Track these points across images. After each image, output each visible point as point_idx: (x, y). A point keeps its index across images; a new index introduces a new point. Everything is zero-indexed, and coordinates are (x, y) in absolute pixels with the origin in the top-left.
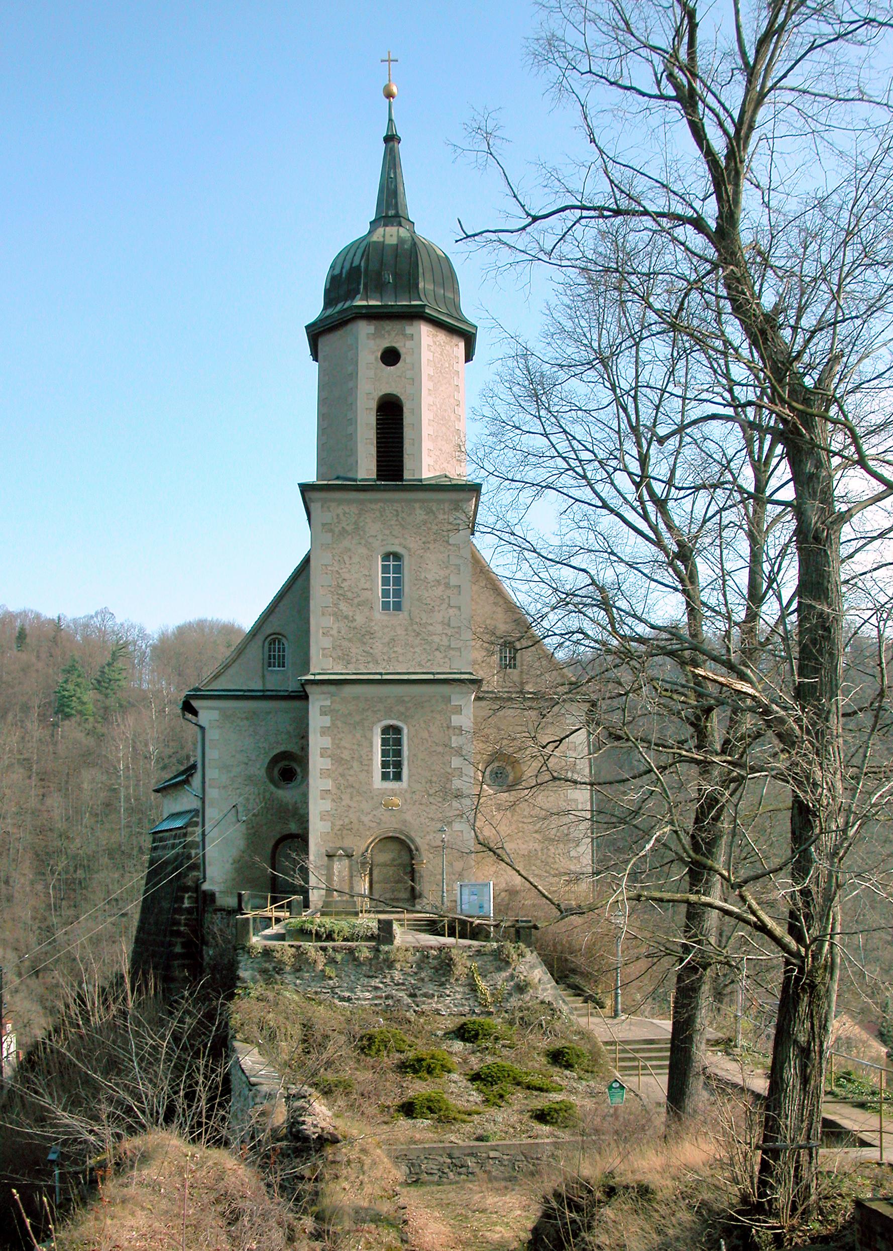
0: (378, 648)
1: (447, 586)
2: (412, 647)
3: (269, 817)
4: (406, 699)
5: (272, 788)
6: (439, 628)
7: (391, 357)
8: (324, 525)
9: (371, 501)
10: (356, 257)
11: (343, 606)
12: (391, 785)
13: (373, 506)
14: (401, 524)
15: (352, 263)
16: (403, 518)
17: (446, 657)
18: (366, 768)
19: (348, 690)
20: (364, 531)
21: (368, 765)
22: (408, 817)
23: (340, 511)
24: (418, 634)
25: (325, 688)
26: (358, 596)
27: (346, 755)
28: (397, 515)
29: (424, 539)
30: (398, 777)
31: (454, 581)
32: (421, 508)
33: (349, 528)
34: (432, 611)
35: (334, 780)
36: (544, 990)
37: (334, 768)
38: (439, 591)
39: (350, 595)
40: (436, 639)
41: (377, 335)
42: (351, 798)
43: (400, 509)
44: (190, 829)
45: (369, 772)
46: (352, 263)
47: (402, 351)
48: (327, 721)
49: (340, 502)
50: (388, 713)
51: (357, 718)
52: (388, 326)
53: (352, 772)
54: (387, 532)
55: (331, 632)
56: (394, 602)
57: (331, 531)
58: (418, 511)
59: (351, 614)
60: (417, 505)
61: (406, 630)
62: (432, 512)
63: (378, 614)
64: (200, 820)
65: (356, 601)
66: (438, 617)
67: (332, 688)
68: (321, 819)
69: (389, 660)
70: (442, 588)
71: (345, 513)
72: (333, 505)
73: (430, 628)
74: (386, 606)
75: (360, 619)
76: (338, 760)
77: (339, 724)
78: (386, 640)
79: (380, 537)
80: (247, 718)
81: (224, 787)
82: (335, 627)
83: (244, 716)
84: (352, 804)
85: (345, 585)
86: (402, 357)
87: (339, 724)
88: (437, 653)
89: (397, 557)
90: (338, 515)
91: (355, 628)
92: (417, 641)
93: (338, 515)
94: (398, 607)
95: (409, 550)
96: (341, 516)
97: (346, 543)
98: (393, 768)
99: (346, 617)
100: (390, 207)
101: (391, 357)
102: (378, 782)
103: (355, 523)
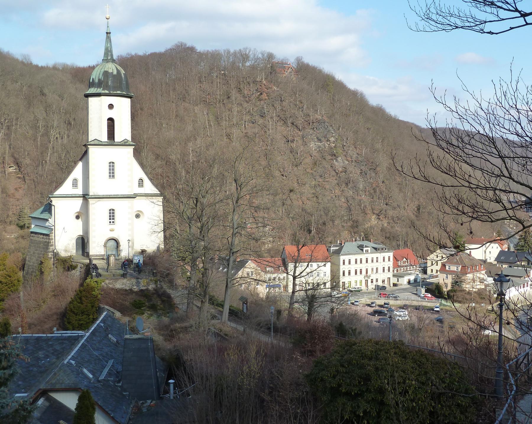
7: (111, 106)
56: (112, 175)
101: (111, 106)
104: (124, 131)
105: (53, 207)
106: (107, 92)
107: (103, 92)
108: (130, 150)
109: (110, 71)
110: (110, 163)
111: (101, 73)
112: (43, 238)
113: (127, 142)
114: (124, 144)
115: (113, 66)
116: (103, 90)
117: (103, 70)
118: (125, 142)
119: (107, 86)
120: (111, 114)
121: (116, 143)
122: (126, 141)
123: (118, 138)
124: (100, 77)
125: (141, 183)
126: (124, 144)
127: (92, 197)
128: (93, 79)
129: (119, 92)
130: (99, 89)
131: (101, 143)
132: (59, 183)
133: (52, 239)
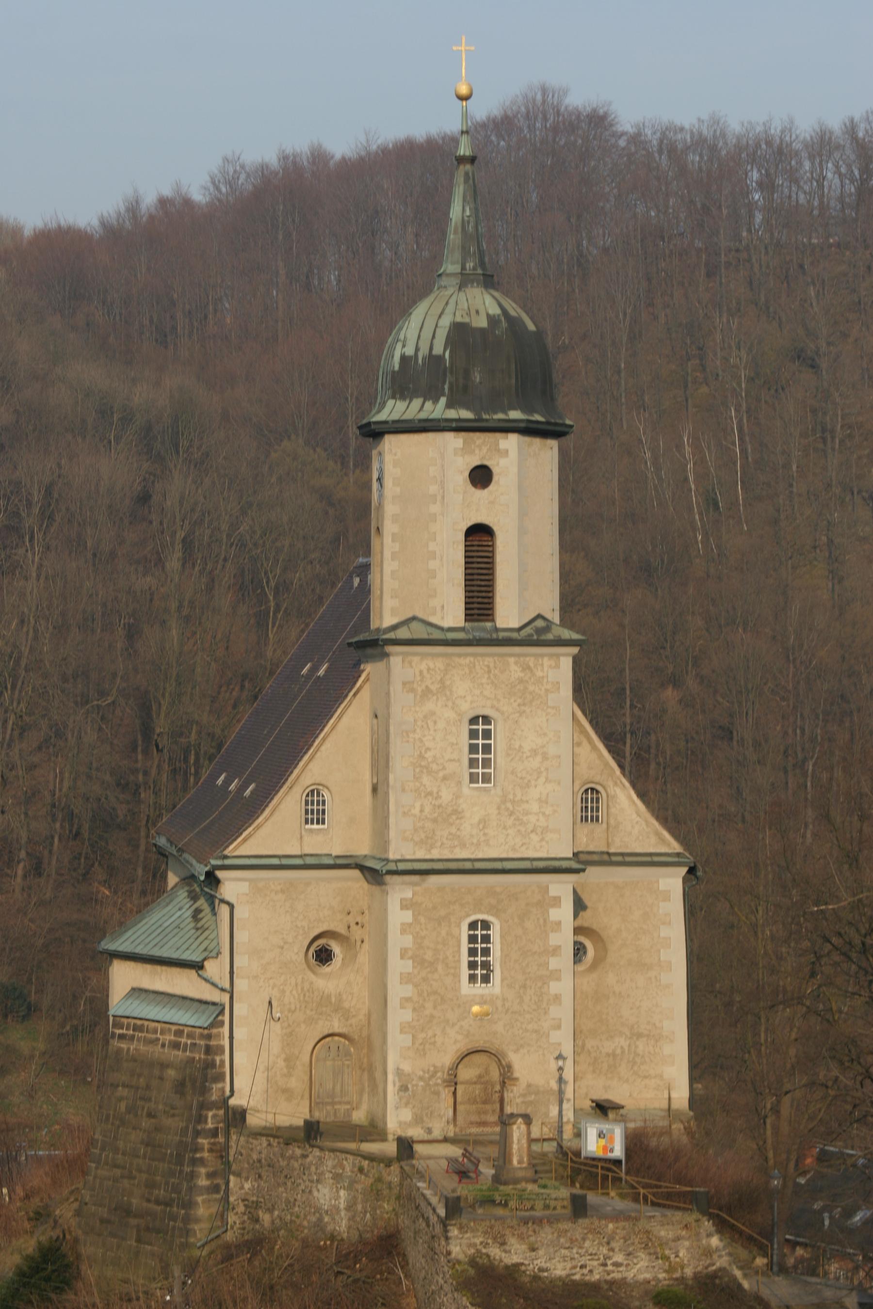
1: (545, 757)
2: (505, 828)
3: (308, 1012)
4: (498, 890)
5: (312, 976)
6: (535, 807)
7: (481, 476)
8: (404, 684)
9: (459, 655)
10: (435, 342)
11: (426, 780)
12: (479, 988)
13: (462, 661)
14: (493, 683)
15: (431, 348)
16: (495, 676)
17: (542, 840)
18: (452, 971)
19: (434, 879)
20: (451, 691)
22: (499, 1027)
23: (423, 666)
24: (511, 814)
25: (407, 878)
26: (444, 768)
27: (429, 956)
28: (489, 672)
29: (519, 701)
30: (486, 979)
31: (552, 750)
32: (516, 663)
33: (434, 688)
34: (528, 785)
35: (416, 986)
36: (720, 1257)
37: (416, 972)
38: (535, 763)
39: (434, 767)
40: (533, 819)
41: (466, 450)
42: (435, 1007)
43: (492, 665)
44: (214, 1031)
45: (457, 976)
46: (431, 348)
47: (495, 470)
48: (407, 916)
49: (424, 656)
51: (443, 912)
54: (477, 692)
55: (413, 811)
57: (413, 690)
58: (513, 667)
59: (435, 790)
60: (512, 660)
61: (499, 808)
62: (529, 668)
63: (467, 789)
64: (226, 1018)
65: (441, 774)
67: (415, 878)
68: (401, 1032)
69: (478, 844)
70: (539, 758)
71: (429, 669)
72: (416, 659)
73: (525, 806)
74: (473, 778)
75: (446, 795)
76: (419, 961)
77: (422, 920)
78: (476, 820)
79: (469, 698)
80: (282, 891)
81: (256, 977)
82: (418, 805)
83: (279, 888)
85: (429, 755)
86: (495, 478)
87: (422, 920)
88: (533, 836)
89: (486, 720)
90: (421, 672)
91: (440, 806)
92: (510, 822)
93: (421, 672)
95: (502, 713)
96: (425, 672)
97: (430, 705)
98: (480, 971)
99: (430, 794)
101: (481, 476)
103: (442, 681)
105: (224, 910)
106: (466, 414)
107: (452, 414)
108: (557, 670)
109: (481, 322)
110: (474, 720)
114: (534, 636)
115: (488, 300)
116: (449, 405)
118: (539, 631)
119: (465, 388)
120: (481, 507)
121: (502, 635)
122: (540, 623)
123: (508, 614)
124: (438, 350)
125: (590, 804)
126: (534, 636)
127: (402, 866)
128: (404, 358)
129: (515, 414)
131: (437, 635)
132: (249, 811)
133: (221, 1050)
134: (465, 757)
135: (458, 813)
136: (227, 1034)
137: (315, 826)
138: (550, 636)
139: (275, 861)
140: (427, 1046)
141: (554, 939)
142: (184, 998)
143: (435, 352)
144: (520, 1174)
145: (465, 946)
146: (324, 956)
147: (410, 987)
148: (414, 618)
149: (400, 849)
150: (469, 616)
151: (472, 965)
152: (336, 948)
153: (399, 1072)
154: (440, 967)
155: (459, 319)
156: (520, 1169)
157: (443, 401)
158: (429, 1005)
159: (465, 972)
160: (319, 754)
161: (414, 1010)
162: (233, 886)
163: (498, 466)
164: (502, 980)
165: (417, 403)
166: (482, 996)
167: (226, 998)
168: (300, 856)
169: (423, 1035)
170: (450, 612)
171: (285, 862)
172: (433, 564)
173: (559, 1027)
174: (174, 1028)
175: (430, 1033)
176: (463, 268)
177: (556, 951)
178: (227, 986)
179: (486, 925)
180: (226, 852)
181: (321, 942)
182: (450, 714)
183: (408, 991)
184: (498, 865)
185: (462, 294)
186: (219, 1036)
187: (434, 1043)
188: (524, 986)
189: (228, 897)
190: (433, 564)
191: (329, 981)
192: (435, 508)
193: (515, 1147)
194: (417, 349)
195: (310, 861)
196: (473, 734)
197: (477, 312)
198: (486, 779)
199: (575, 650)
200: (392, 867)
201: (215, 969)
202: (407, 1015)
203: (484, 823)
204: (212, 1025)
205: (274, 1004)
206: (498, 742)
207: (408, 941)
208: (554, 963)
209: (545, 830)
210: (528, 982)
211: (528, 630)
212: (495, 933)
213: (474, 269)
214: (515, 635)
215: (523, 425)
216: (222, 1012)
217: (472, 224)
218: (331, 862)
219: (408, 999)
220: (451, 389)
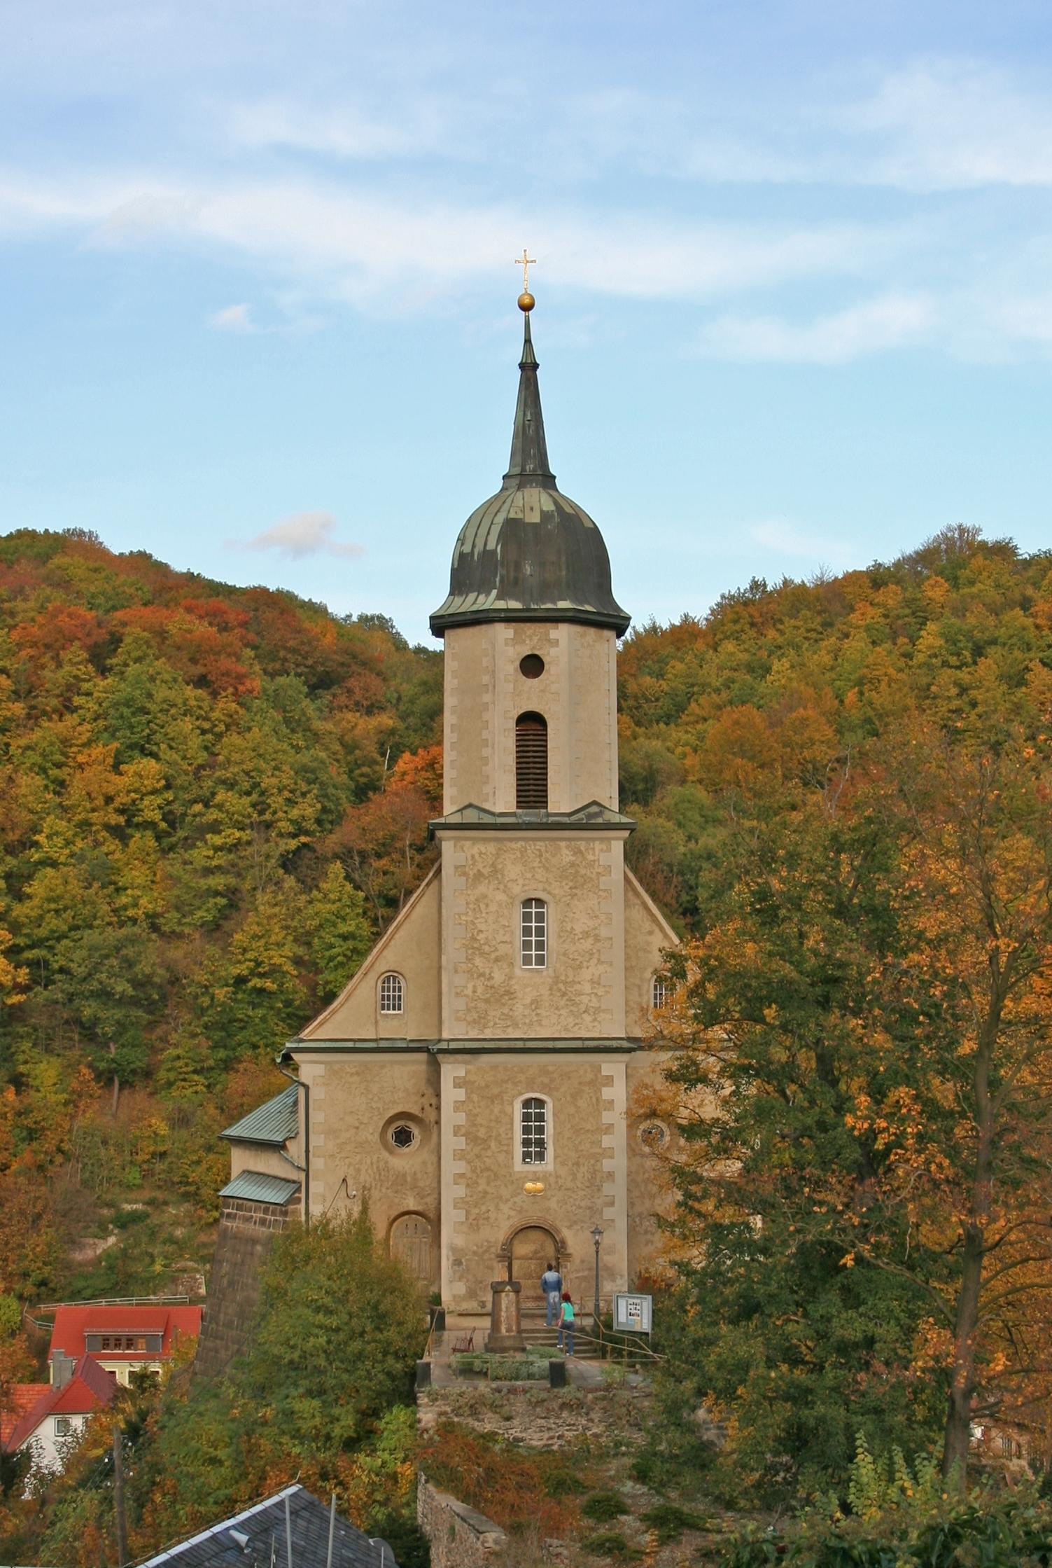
0: (519, 1010)
1: (597, 939)
2: (557, 1008)
3: (384, 1190)
4: (551, 1069)
6: (587, 988)
7: (532, 666)
8: (456, 867)
9: (511, 840)
10: (490, 538)
11: (478, 961)
12: (536, 1166)
13: (513, 845)
14: (544, 866)
15: (485, 544)
16: (547, 859)
17: (595, 1020)
19: (485, 1058)
20: (503, 875)
21: (508, 1145)
22: (553, 1204)
23: (475, 851)
24: (564, 994)
25: (459, 1057)
26: (496, 950)
27: (482, 1133)
28: (541, 856)
29: (571, 884)
30: (541, 1156)
31: (604, 932)
32: (567, 847)
33: (485, 871)
34: (580, 967)
35: (469, 1162)
38: (587, 944)
39: (486, 948)
40: (585, 999)
41: (516, 640)
42: (488, 1183)
43: (543, 849)
45: (510, 1153)
46: (485, 544)
47: (545, 659)
48: (461, 1094)
49: (475, 840)
50: (530, 1086)
51: (496, 1091)
52: (530, 628)
53: (489, 1153)
54: (529, 875)
55: (466, 992)
57: (465, 874)
58: (565, 851)
59: (487, 971)
60: (563, 844)
61: (551, 989)
62: (581, 852)
63: (520, 970)
64: (303, 1195)
65: (493, 956)
66: (586, 974)
67: (467, 1057)
69: (531, 1024)
70: (591, 940)
71: (480, 853)
72: (468, 843)
73: (577, 987)
74: (527, 960)
75: (498, 977)
76: (472, 1138)
77: (475, 1098)
78: (528, 1001)
79: (521, 882)
80: (357, 1074)
81: (332, 1156)
82: (470, 986)
83: (354, 1070)
84: (488, 1189)
85: (481, 936)
86: (546, 667)
87: (475, 1098)
88: (585, 1016)
89: (540, 902)
90: (473, 856)
91: (492, 987)
92: (563, 1003)
93: (473, 856)
94: (540, 960)
95: (554, 896)
96: (477, 856)
97: (482, 888)
98: (535, 1148)
99: (482, 975)
100: (530, 461)
101: (532, 666)
102: (518, 1165)
103: (493, 865)
104: (584, 772)
106: (514, 604)
107: (501, 605)
108: (610, 853)
109: (535, 518)
110: (527, 903)
111: (496, 530)
112: (263, 1222)
113: (599, 814)
114: (586, 821)
116: (499, 598)
117: (500, 519)
118: (590, 816)
119: (516, 582)
121: (551, 819)
122: (594, 809)
123: (561, 800)
126: (586, 821)
127: (453, 1045)
129: (562, 604)
130: (482, 598)
131: (488, 819)
134: (520, 938)
135: (510, 993)
136: (303, 1212)
137: (391, 1012)
138: (600, 820)
139: (350, 1045)
140: (481, 1222)
141: (607, 1117)
142: (276, 1178)
143: (488, 548)
144: (508, 1343)
145: (518, 1125)
146: (403, 1137)
147: (463, 1163)
148: (470, 806)
149: (452, 1030)
150: (520, 804)
151: (526, 1143)
152: (415, 1131)
153: (454, 1249)
154: (493, 1144)
155: (512, 515)
156: (509, 1337)
157: (494, 592)
158: (482, 1181)
159: (519, 1150)
160: (393, 942)
161: (468, 1185)
162: (310, 1069)
163: (549, 655)
164: (555, 1158)
165: (472, 596)
166: (535, 1173)
167: (302, 1176)
168: (375, 1040)
169: (477, 1211)
170: (504, 800)
171: (358, 1045)
172: (486, 752)
173: (612, 1204)
174: (263, 1206)
175: (484, 1209)
176: (523, 469)
177: (609, 1129)
178: (303, 1165)
179: (540, 1103)
180: (301, 1036)
181: (400, 1123)
182: (501, 897)
183: (461, 1167)
184: (550, 1045)
185: (519, 494)
186: (295, 1212)
187: (488, 1218)
188: (577, 1164)
189: (303, 1079)
190: (486, 752)
191: (406, 1160)
192: (487, 698)
193: (503, 1314)
194: (474, 546)
195: (383, 1044)
196: (527, 917)
197: (532, 509)
198: (540, 960)
199: (626, 834)
200: (444, 1045)
201: (295, 1149)
202: (461, 1191)
203: (536, 1003)
204: (288, 1202)
205: (350, 1182)
206: (551, 925)
207: (461, 1118)
208: (607, 1141)
209: (598, 1010)
210: (581, 1160)
211: (580, 815)
212: (548, 1111)
213: (534, 470)
214: (566, 820)
215: (570, 614)
216: (298, 1190)
217: (532, 428)
218: (404, 1045)
219: (462, 1175)
220: (502, 581)
